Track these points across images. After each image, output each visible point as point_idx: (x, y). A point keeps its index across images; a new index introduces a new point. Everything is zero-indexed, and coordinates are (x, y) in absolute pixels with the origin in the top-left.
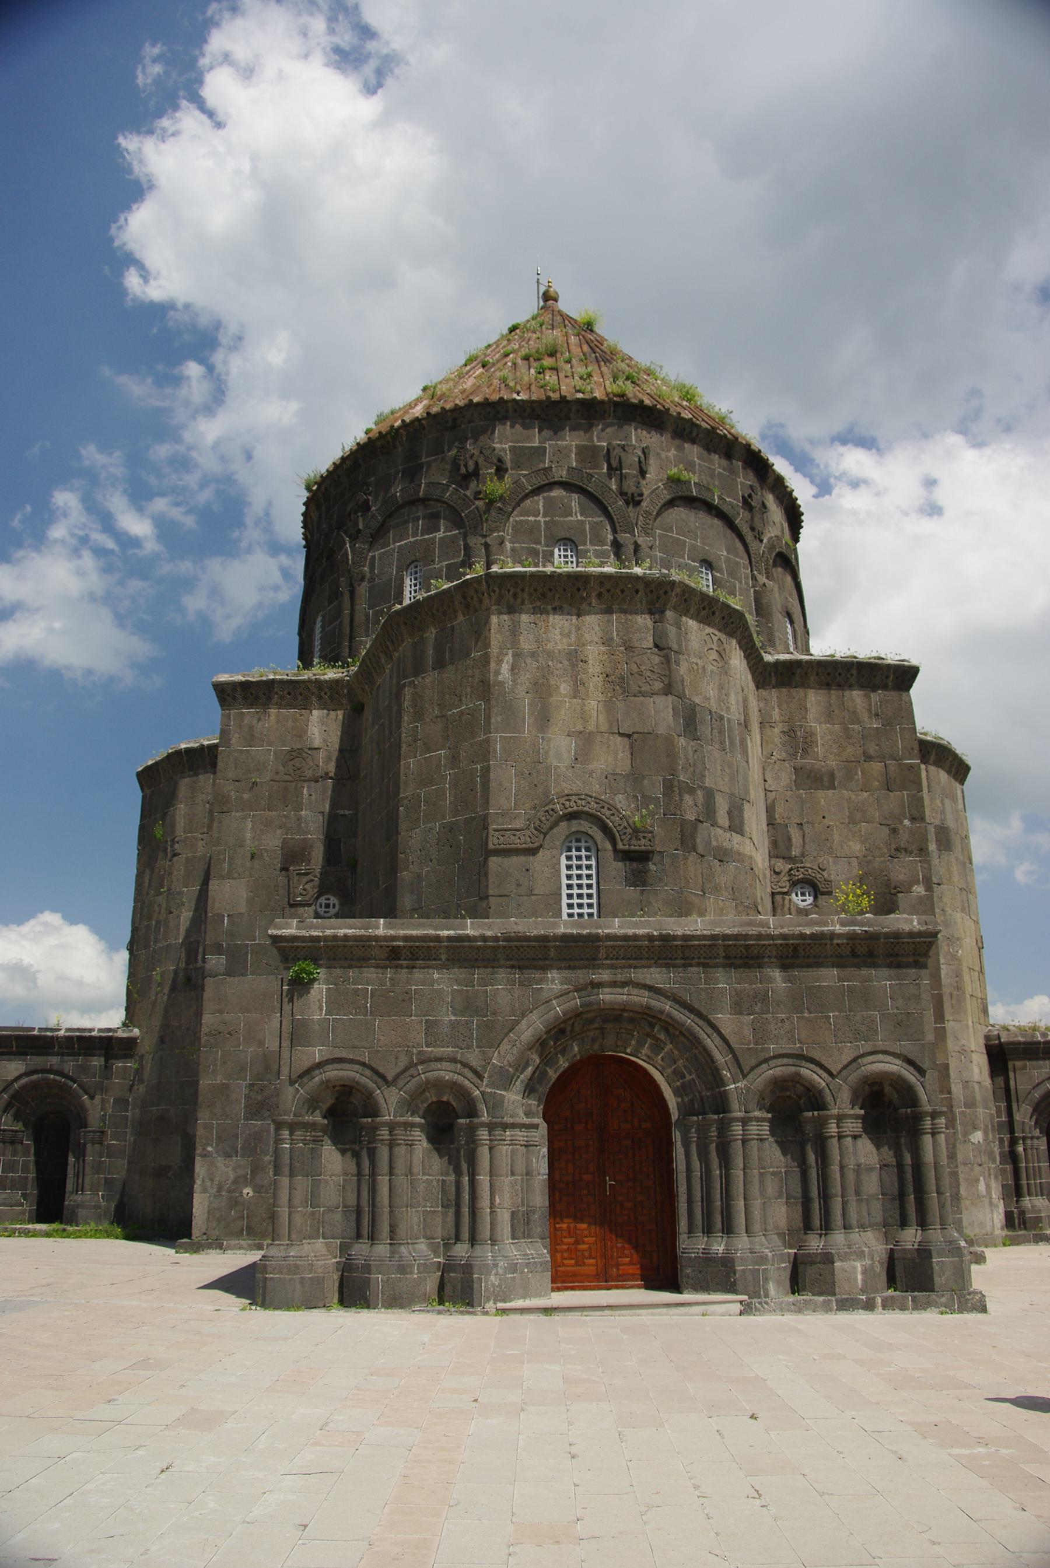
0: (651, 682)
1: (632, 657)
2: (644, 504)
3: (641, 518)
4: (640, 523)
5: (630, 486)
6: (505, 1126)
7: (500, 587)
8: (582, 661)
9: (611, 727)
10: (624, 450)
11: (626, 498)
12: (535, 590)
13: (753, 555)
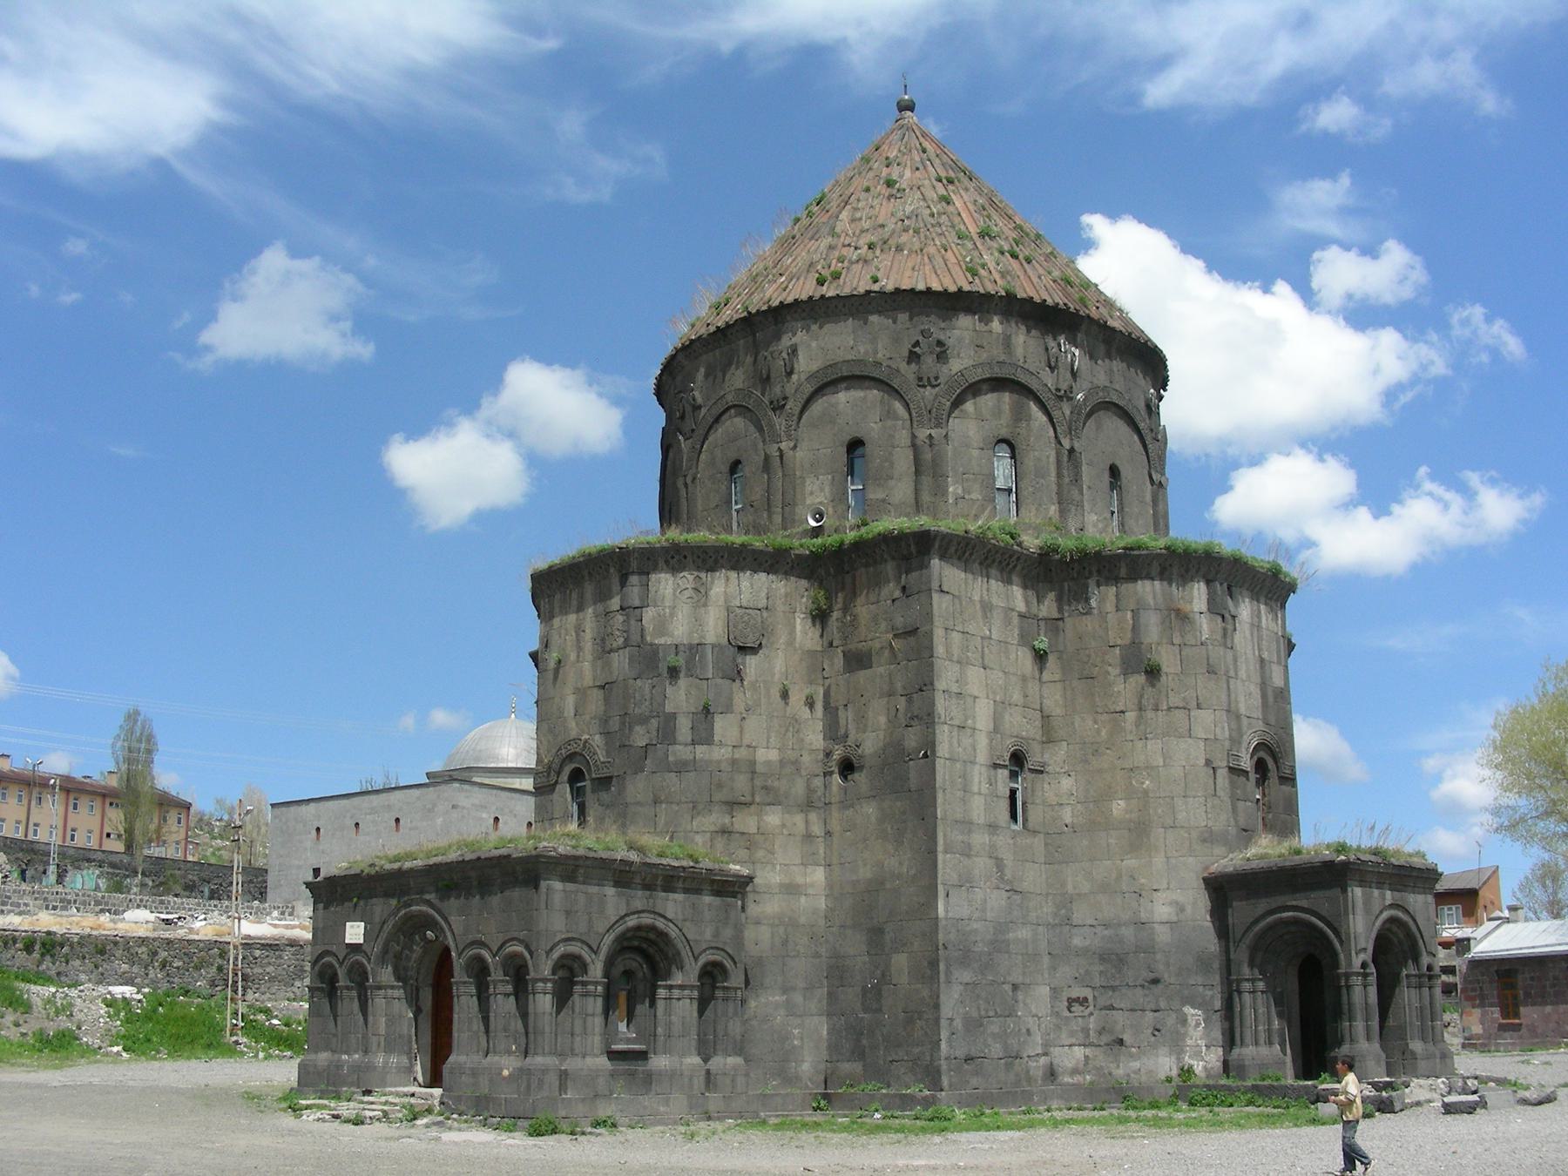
2: (787, 407)
6: (379, 988)
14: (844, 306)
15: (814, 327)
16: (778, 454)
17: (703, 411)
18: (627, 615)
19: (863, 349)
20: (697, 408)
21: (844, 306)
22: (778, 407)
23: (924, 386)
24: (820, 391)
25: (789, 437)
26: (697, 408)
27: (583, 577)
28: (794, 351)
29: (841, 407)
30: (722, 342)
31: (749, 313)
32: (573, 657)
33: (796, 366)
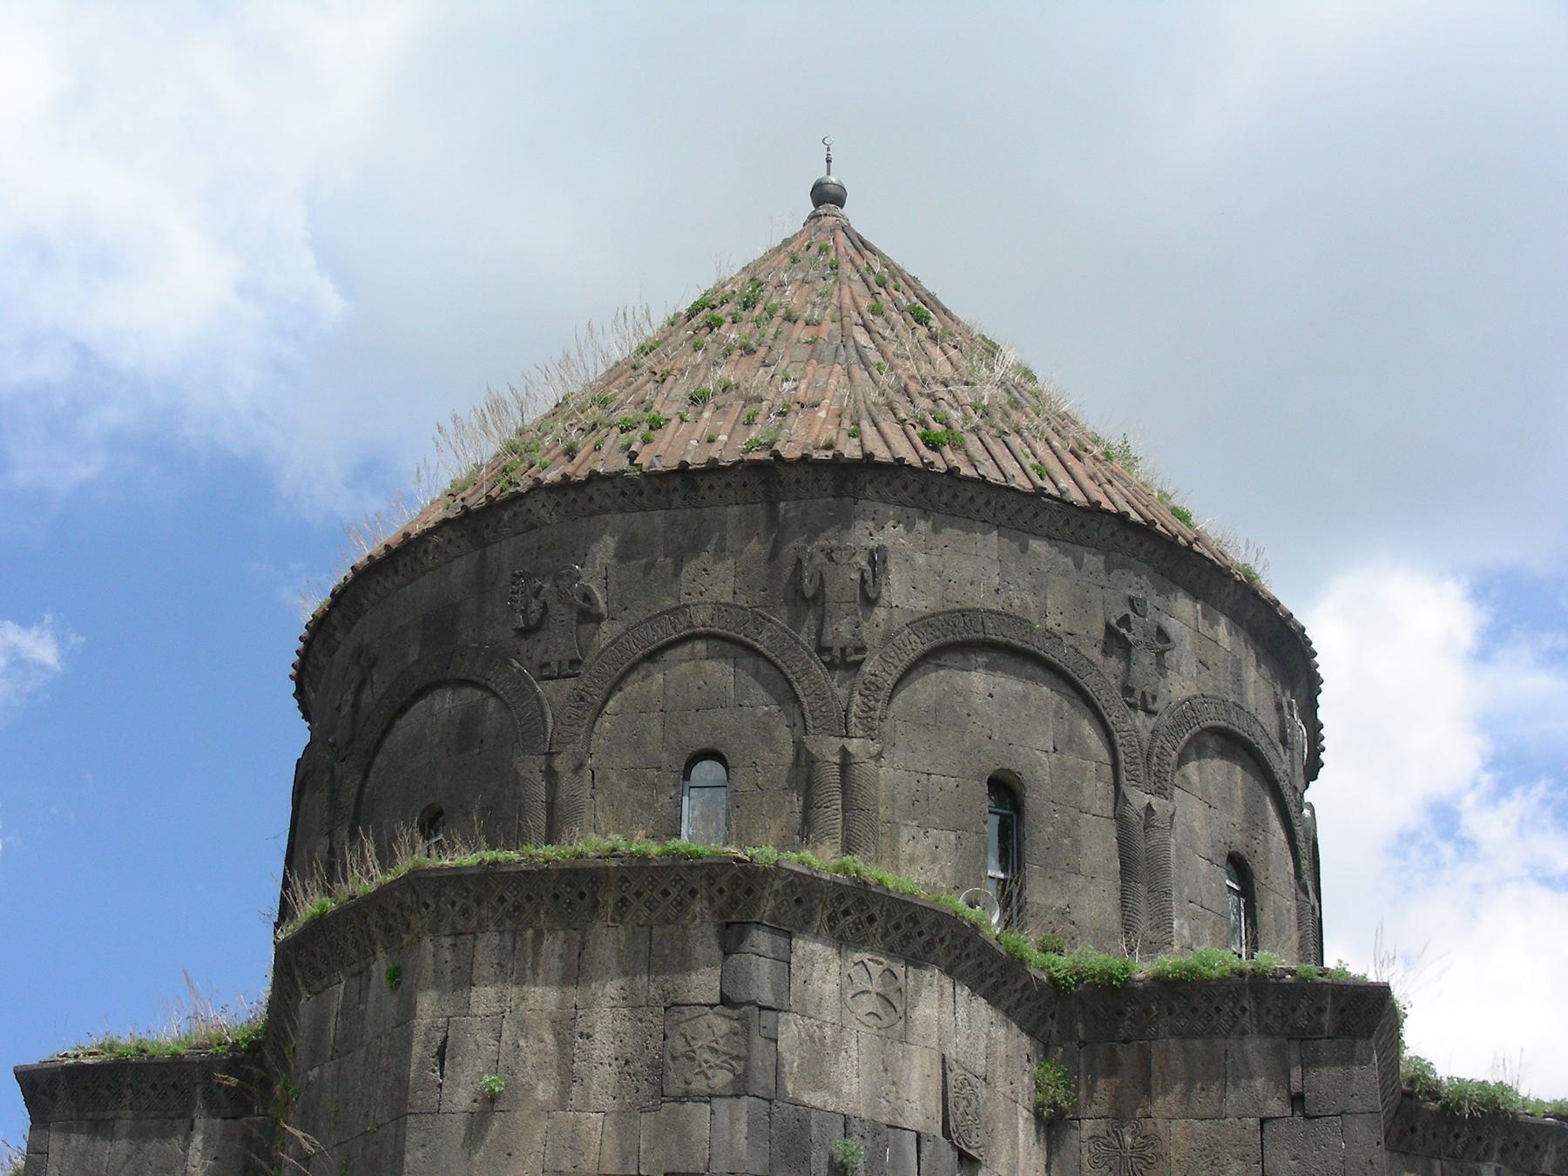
0: (709, 1073)
1: (678, 1023)
2: (867, 668)
3: (857, 698)
4: (854, 708)
5: (841, 630)
7: (437, 896)
8: (581, 1036)
9: (624, 1160)
10: (831, 559)
11: (827, 658)
12: (502, 900)
13: (1121, 749)
14: (988, 503)
15: (922, 526)
16: (837, 759)
17: (606, 632)
18: (744, 1020)
19: (1020, 598)
20: (589, 616)
21: (988, 503)
22: (846, 662)
23: (1133, 706)
24: (931, 657)
25: (870, 733)
26: (589, 616)
27: (595, 906)
28: (877, 559)
29: (977, 701)
30: (677, 499)
31: (777, 456)
32: (544, 1091)
33: (884, 590)
